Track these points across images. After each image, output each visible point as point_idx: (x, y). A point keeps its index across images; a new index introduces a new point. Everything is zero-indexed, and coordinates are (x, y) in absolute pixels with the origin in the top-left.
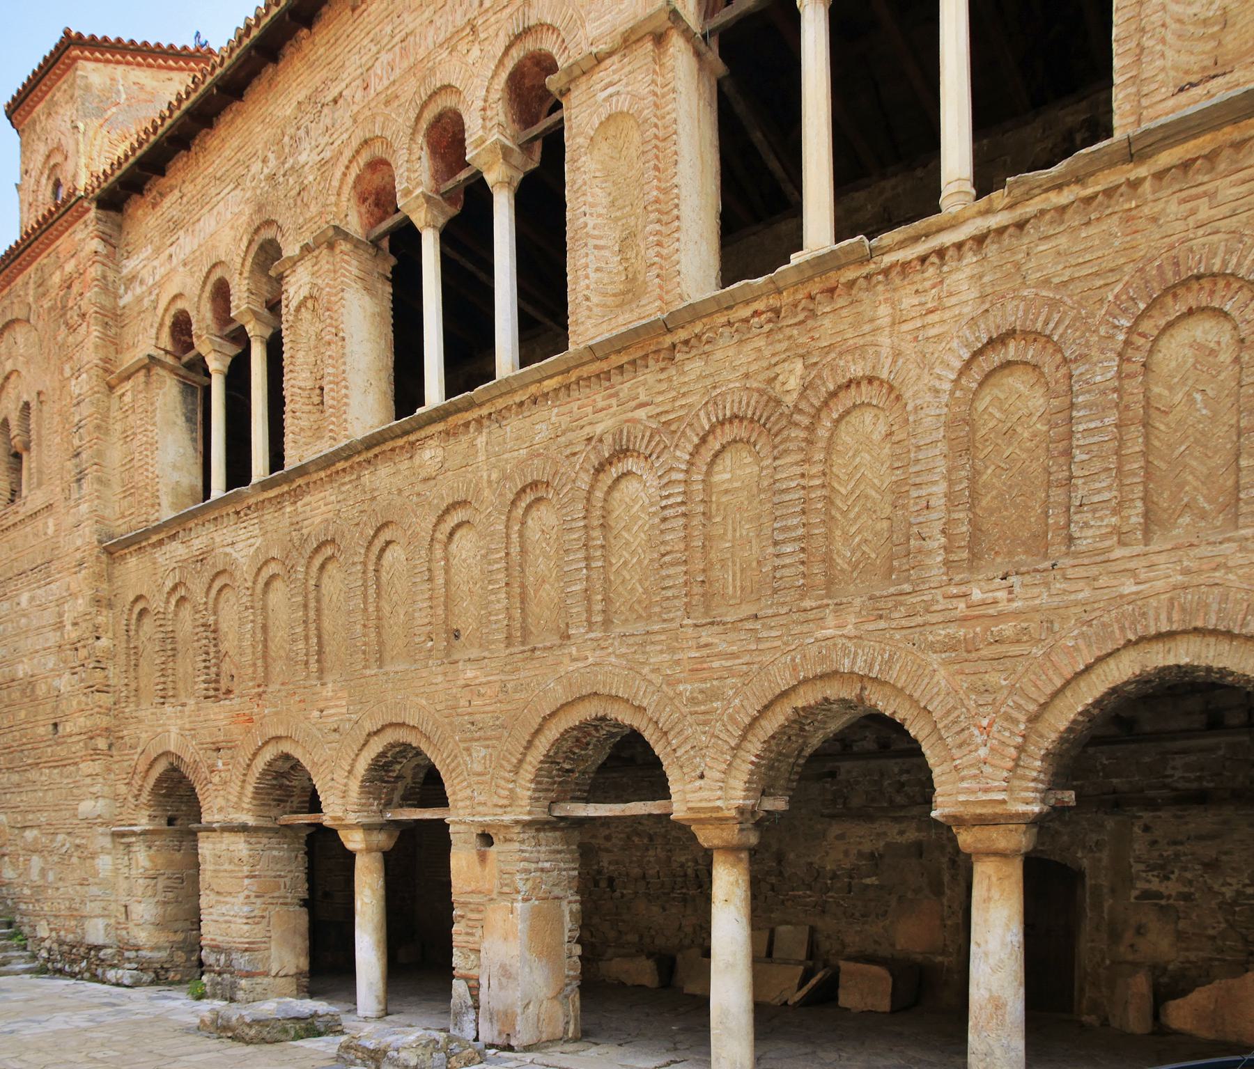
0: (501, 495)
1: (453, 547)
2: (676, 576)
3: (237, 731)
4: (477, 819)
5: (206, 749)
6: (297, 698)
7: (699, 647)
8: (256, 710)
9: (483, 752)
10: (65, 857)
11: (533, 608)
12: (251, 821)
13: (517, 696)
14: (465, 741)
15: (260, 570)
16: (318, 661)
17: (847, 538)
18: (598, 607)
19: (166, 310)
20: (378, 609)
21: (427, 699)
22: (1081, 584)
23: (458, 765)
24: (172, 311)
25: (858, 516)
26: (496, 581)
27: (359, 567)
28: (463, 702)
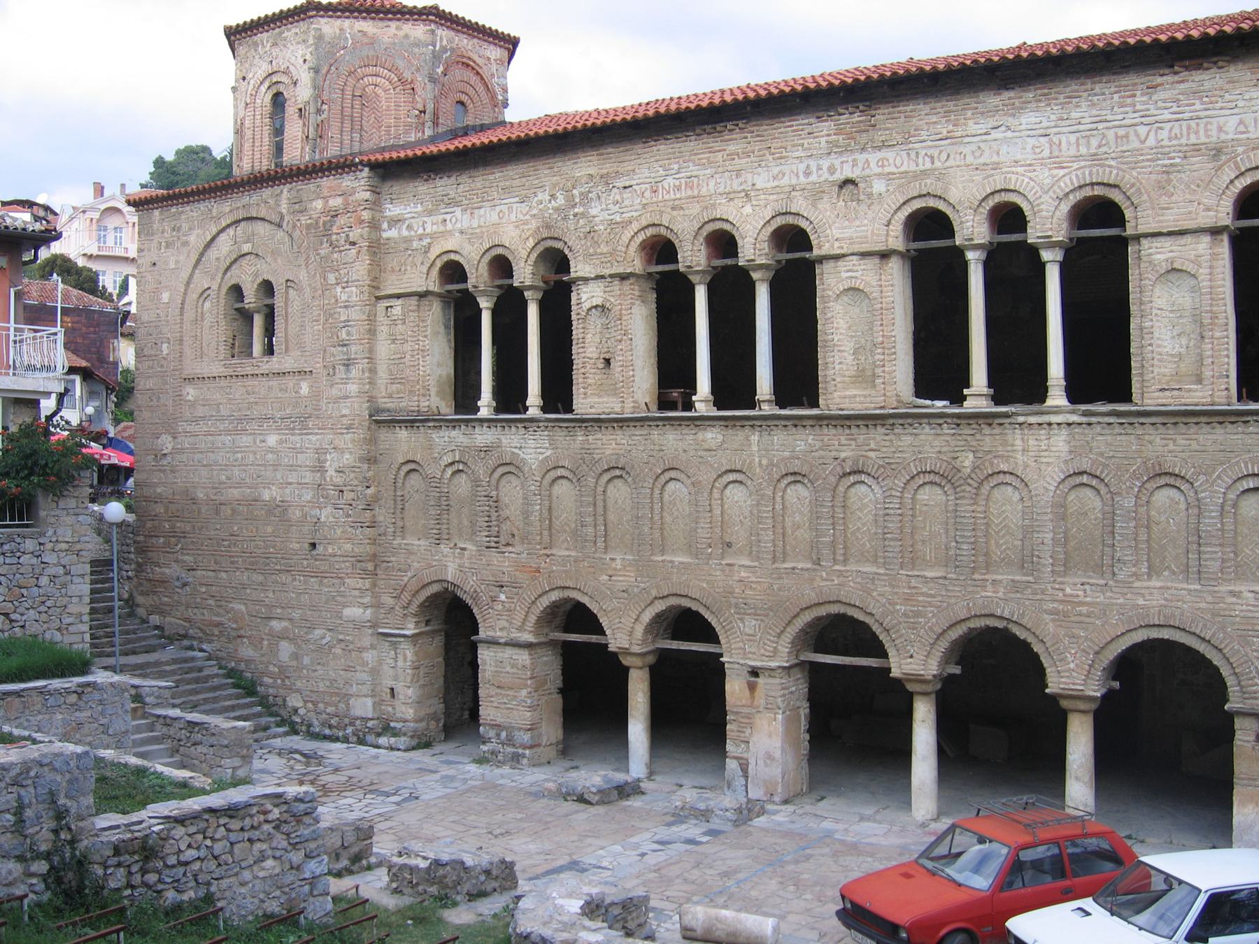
0: (769, 474)
2: (894, 547)
5: (488, 585)
7: (910, 588)
9: (754, 622)
13: (782, 593)
14: (739, 614)
17: (998, 545)
21: (707, 584)
22: (1119, 596)
23: (733, 627)
25: (1003, 536)
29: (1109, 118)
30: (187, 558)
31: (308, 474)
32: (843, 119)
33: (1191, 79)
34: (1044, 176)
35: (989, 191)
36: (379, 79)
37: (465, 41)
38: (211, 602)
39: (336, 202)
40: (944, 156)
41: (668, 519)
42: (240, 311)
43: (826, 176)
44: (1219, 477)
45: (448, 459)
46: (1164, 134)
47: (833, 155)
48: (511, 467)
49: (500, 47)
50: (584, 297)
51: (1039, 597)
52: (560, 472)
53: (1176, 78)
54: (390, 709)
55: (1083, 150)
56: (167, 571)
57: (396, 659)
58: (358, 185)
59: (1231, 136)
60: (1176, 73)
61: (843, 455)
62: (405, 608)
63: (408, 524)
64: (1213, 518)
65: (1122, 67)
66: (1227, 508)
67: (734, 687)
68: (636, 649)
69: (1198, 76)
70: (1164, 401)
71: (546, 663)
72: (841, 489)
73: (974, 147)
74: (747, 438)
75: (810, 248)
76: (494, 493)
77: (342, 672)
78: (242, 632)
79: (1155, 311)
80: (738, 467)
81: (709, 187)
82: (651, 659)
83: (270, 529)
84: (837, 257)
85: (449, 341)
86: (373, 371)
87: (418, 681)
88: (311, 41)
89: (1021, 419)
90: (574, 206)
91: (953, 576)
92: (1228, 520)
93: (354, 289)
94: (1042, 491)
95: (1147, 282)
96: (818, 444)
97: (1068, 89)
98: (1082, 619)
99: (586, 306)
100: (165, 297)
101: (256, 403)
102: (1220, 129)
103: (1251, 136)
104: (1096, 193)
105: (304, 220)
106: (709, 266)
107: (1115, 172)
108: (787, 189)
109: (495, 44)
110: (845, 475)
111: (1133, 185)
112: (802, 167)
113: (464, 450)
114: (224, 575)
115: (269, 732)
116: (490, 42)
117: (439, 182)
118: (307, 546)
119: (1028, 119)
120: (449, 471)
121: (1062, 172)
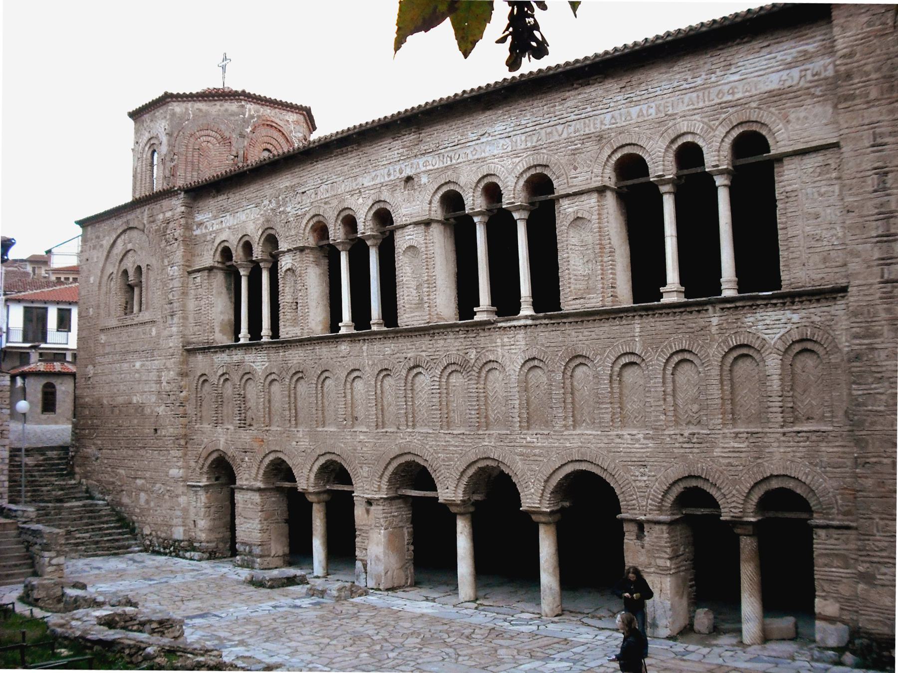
1: (355, 384)
3: (256, 445)
4: (366, 496)
6: (285, 435)
8: (265, 437)
10: (160, 496)
11: (386, 414)
12: (262, 486)
15: (268, 376)
16: (295, 420)
18: (411, 419)
19: (220, 244)
20: (322, 403)
22: (556, 441)
24: (222, 245)
26: (372, 403)
27: (314, 385)
28: (359, 448)
29: (542, 122)
30: (99, 442)
31: (154, 385)
32: (406, 138)
33: (584, 91)
34: (508, 163)
35: (480, 176)
36: (210, 138)
37: (269, 111)
38: (109, 469)
39: (169, 214)
40: (457, 156)
41: (326, 403)
42: (129, 285)
43: (398, 175)
44: (608, 356)
45: (220, 372)
46: (572, 129)
47: (401, 162)
48: (248, 376)
49: (296, 113)
50: (283, 263)
51: (512, 444)
52: (273, 377)
53: (577, 92)
54: (193, 534)
55: (529, 145)
56: (89, 450)
57: (196, 502)
58: (177, 205)
59: (607, 127)
60: (576, 89)
61: (409, 355)
62: (201, 469)
63: (204, 415)
64: (605, 384)
65: (548, 88)
66: (615, 377)
67: (359, 512)
68: (311, 490)
69: (588, 90)
70: (573, 307)
71: (274, 502)
72: (410, 378)
73: (472, 149)
74: (361, 348)
75: (392, 222)
76: (242, 392)
77: (168, 511)
78: (123, 488)
79: (570, 247)
80: (357, 368)
81: (342, 188)
82: (325, 497)
83: (136, 421)
84: (403, 227)
85: (230, 298)
86: (185, 318)
87: (209, 516)
88: (168, 117)
89: (500, 325)
90: (279, 207)
91: (468, 433)
92: (616, 385)
93: (176, 267)
94: (513, 372)
95: (564, 227)
96: (396, 349)
97: (520, 106)
98: (536, 458)
99: (284, 269)
100: (92, 280)
101: (132, 342)
102: (602, 123)
103: (619, 125)
104: (537, 172)
105: (154, 227)
106: (347, 239)
107: (546, 156)
108: (379, 186)
109: (292, 112)
110: (411, 369)
111: (556, 164)
112: (386, 170)
113: (228, 365)
114: (115, 451)
115: (129, 550)
116: (288, 111)
117: (220, 198)
118: (153, 431)
119: (499, 127)
120: (222, 380)
121: (518, 160)
